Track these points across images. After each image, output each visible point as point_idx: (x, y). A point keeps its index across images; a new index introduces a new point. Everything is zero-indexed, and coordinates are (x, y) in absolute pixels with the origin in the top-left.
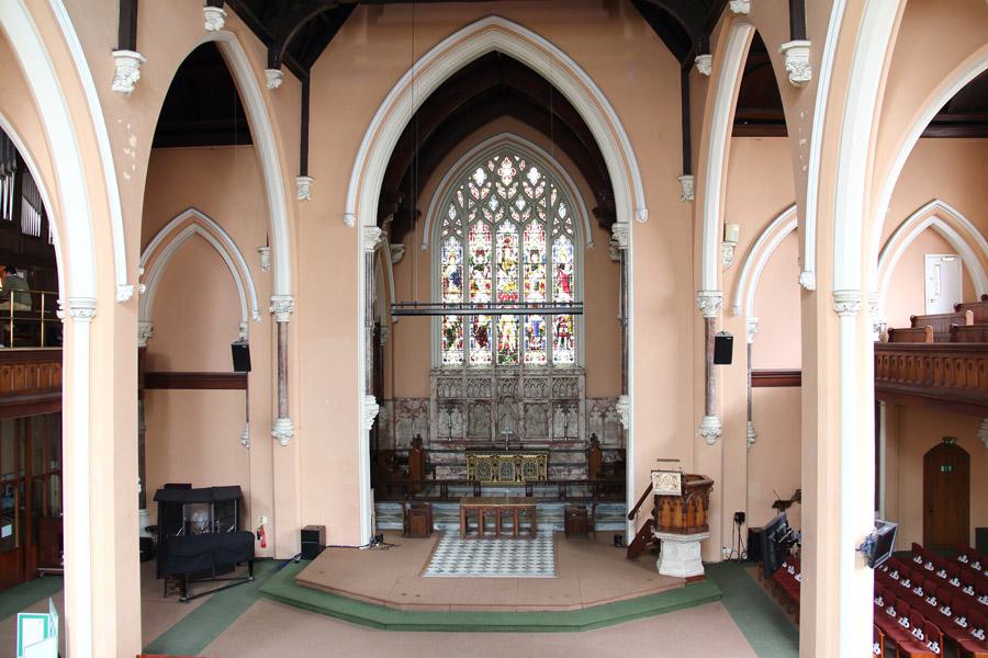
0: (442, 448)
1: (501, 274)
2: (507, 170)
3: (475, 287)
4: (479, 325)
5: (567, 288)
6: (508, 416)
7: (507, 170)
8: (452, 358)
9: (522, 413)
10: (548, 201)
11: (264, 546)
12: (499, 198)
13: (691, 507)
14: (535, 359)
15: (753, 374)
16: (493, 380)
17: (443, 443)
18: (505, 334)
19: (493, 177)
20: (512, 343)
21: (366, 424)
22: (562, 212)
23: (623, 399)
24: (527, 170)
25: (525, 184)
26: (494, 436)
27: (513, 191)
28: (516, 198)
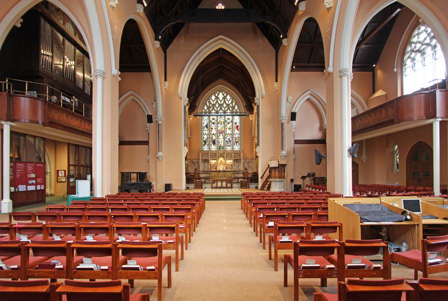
1: (219, 125)
2: (221, 96)
3: (212, 129)
4: (213, 139)
5: (237, 129)
7: (221, 96)
8: (206, 148)
10: (232, 105)
11: (153, 190)
12: (219, 104)
13: (280, 172)
14: (229, 149)
15: (295, 140)
18: (220, 142)
19: (217, 98)
20: (222, 144)
21: (184, 155)
22: (236, 108)
23: (258, 147)
24: (226, 96)
25: (226, 100)
27: (222, 102)
28: (223, 104)
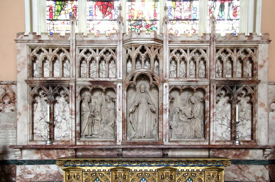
0: (36, 157)
6: (143, 108)
9: (166, 101)
16: (120, 49)
17: (38, 149)
26: (120, 137)
